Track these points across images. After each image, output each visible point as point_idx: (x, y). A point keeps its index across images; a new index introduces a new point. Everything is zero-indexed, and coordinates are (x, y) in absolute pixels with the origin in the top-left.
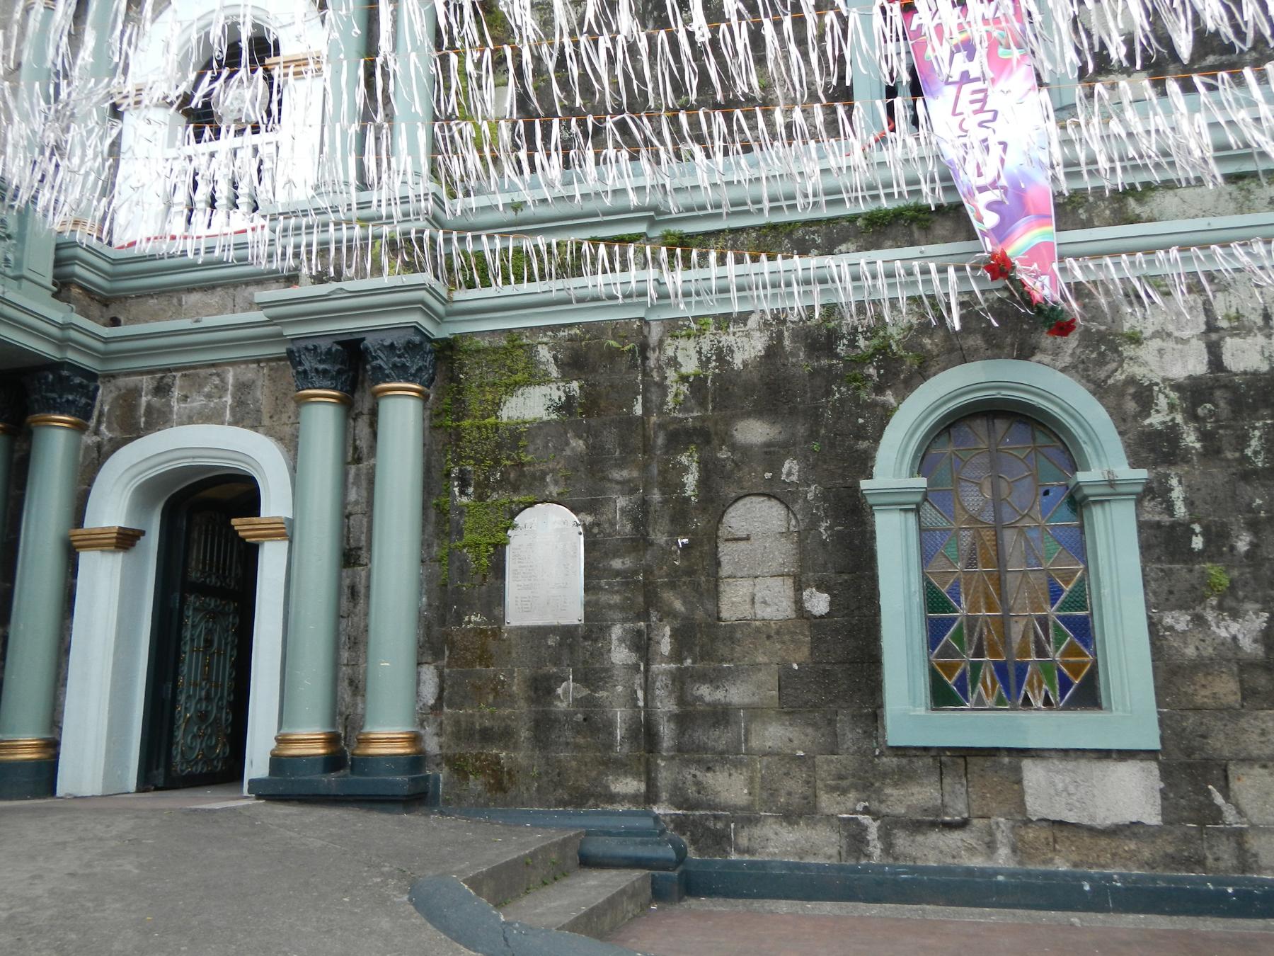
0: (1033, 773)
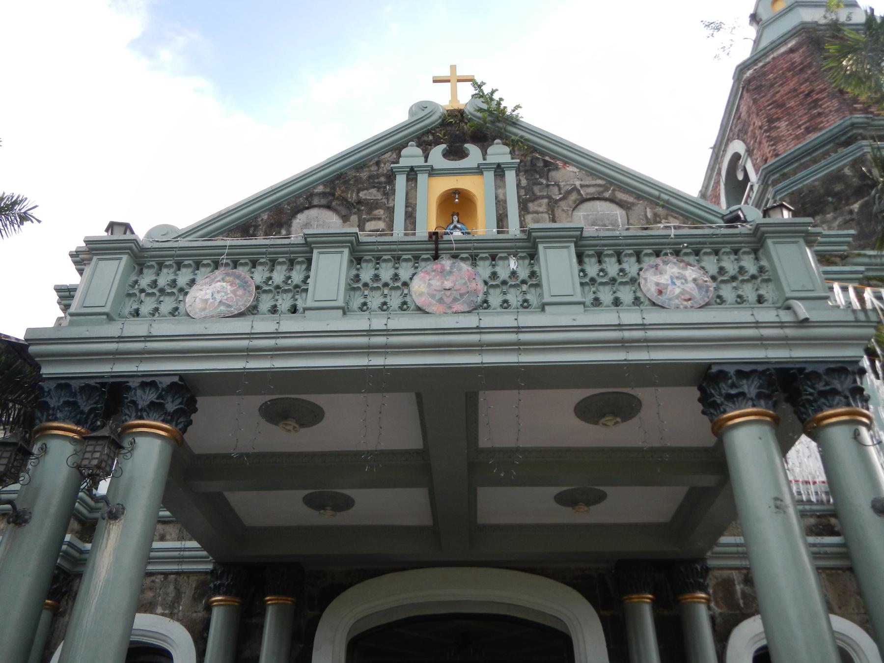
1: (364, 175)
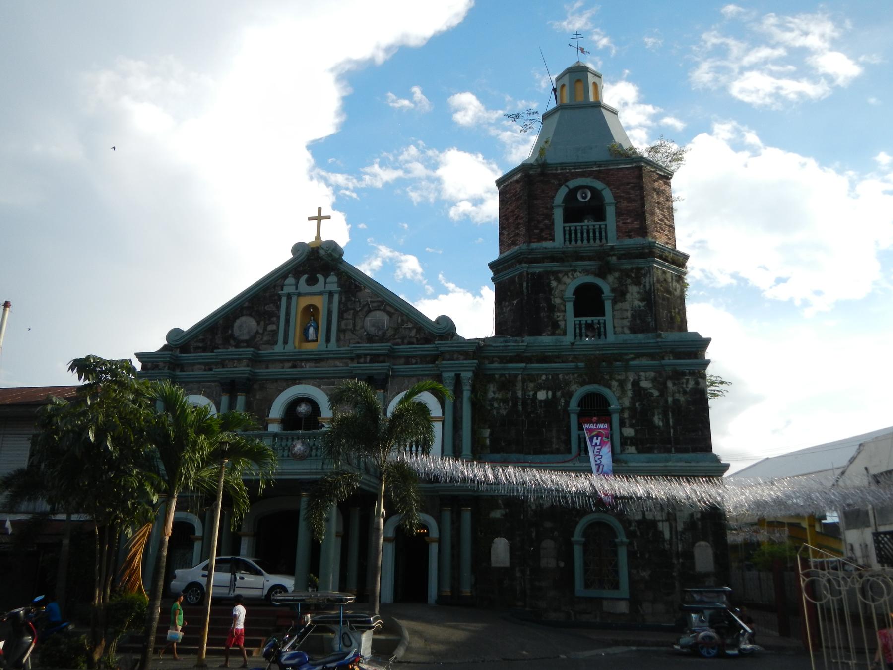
0: (605, 603)
1: (267, 294)
